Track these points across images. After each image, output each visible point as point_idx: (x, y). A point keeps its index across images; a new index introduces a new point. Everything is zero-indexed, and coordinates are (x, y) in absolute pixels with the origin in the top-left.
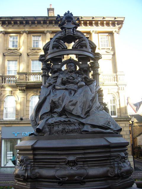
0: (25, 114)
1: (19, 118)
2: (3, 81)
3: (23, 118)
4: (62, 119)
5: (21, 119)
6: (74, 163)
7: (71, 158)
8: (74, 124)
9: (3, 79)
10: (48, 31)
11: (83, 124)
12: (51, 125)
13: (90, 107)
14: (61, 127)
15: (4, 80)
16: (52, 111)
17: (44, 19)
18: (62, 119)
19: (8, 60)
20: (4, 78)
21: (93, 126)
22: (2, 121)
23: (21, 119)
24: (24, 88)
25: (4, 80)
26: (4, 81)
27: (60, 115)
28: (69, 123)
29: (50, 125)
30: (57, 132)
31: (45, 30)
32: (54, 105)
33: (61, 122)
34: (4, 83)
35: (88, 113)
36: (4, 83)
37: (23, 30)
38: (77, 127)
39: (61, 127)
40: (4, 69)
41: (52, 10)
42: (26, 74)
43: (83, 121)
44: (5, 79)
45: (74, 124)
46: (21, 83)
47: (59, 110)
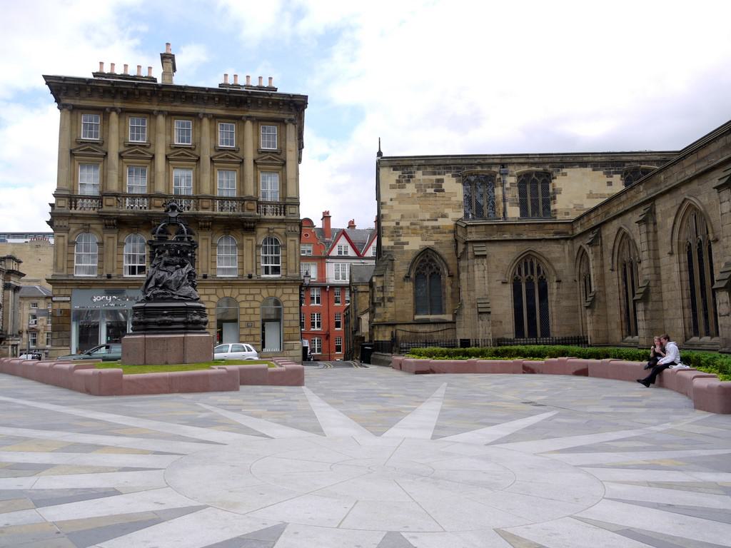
0: (115, 267)
1: (105, 274)
2: (71, 204)
3: (113, 274)
4: (161, 291)
5: (109, 276)
6: (166, 315)
7: (165, 312)
8: (169, 294)
9: (71, 201)
10: (160, 112)
11: (174, 295)
12: (155, 295)
13: (180, 284)
14: (161, 296)
15: (73, 203)
16: (156, 286)
17: (152, 89)
18: (161, 291)
19: (79, 163)
20: (73, 199)
21: (180, 296)
22: (72, 278)
23: (109, 276)
24: (115, 221)
25: (73, 203)
26: (73, 206)
27: (161, 288)
28: (166, 294)
29: (154, 295)
30: (159, 299)
31: (155, 108)
32: (157, 282)
33: (160, 294)
34: (73, 208)
35: (178, 288)
36: (73, 208)
37: (111, 105)
38: (171, 296)
39: (161, 296)
40: (72, 182)
41: (170, 58)
42: (116, 195)
43: (173, 293)
44: (76, 202)
45: (169, 294)
46: (109, 212)
47: (160, 285)
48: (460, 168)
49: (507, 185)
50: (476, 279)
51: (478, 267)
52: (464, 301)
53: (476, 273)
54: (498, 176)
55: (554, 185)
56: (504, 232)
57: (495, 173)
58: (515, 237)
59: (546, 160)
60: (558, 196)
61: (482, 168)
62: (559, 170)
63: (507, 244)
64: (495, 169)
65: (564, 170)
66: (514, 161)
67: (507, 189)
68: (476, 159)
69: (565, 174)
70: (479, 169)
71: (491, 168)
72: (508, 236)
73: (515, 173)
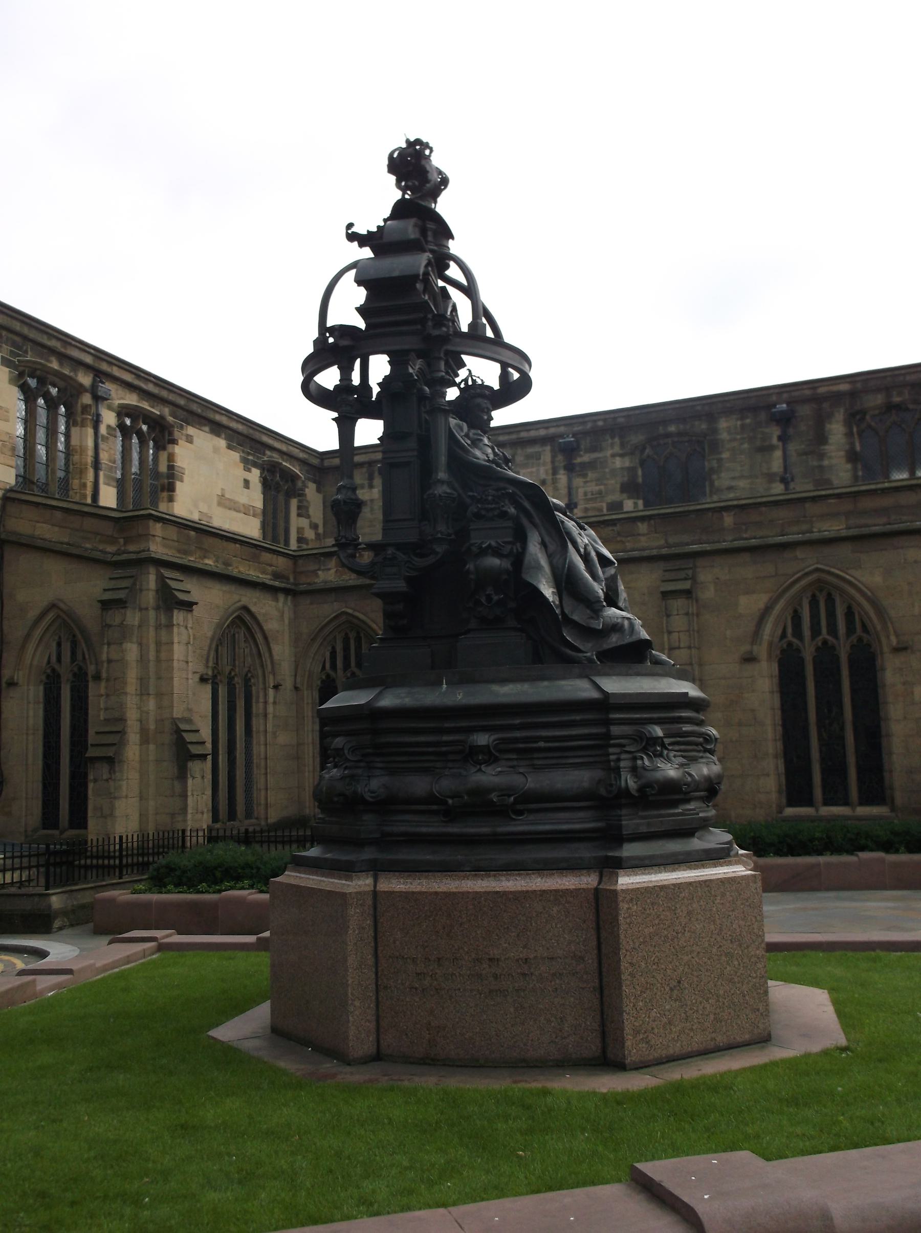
48: (19, 348)
49: (103, 430)
50: (175, 664)
51: (179, 634)
52: (129, 722)
53: (176, 647)
54: (87, 399)
55: (171, 458)
56: (205, 553)
57: (81, 389)
58: (220, 568)
59: (164, 394)
60: (178, 484)
61: (61, 364)
62: (182, 427)
63: (210, 583)
64: (85, 379)
65: (191, 430)
66: (116, 372)
67: (105, 439)
68: (51, 336)
69: (190, 440)
70: (55, 365)
71: (75, 371)
72: (209, 563)
73: (117, 402)
